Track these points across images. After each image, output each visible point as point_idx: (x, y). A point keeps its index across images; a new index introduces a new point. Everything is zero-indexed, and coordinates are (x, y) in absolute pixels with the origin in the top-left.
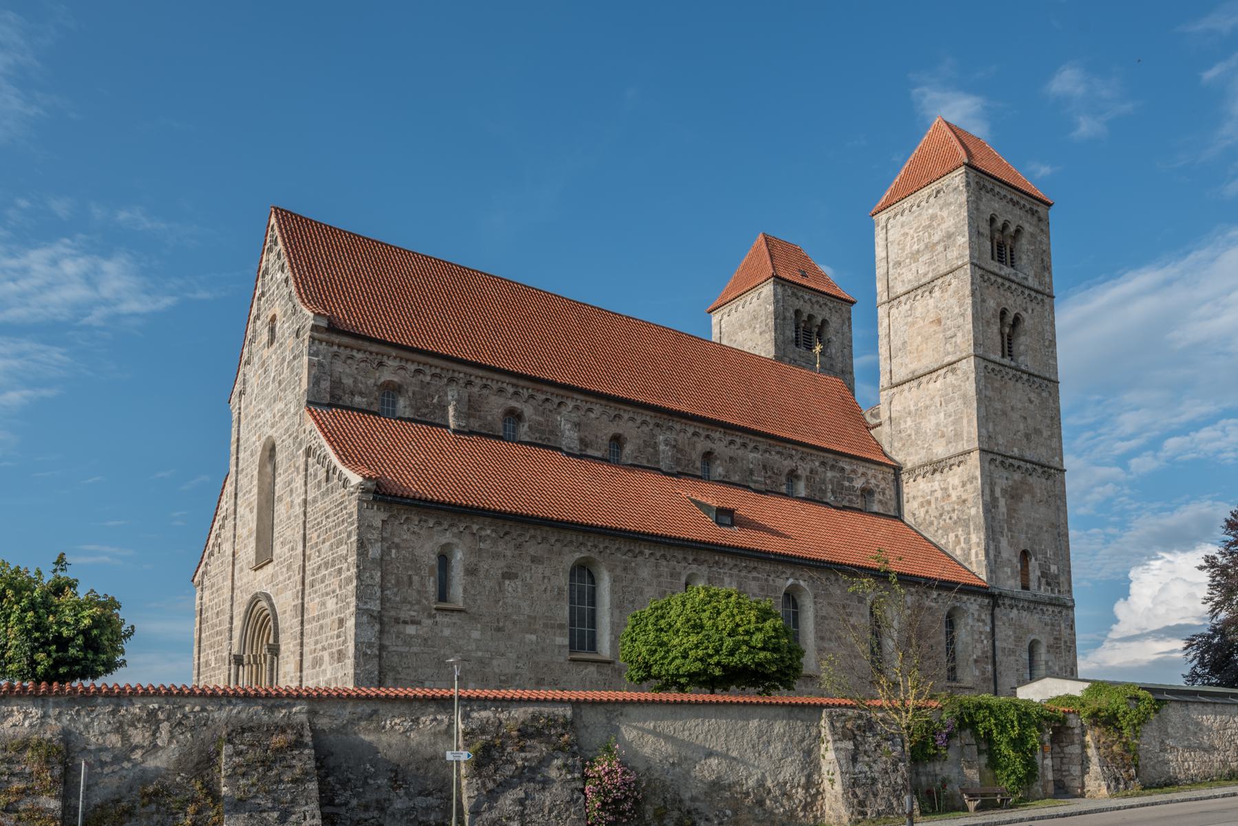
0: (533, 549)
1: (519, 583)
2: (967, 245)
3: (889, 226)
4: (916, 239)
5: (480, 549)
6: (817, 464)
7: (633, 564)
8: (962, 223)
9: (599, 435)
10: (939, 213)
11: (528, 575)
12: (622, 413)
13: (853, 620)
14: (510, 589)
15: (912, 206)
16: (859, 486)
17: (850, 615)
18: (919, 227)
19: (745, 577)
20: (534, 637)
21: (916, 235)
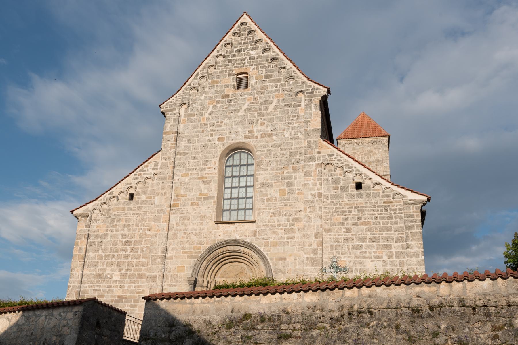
2: (389, 168)
3: (346, 147)
4: (360, 157)
8: (386, 158)
10: (374, 150)
15: (359, 143)
18: (362, 152)
21: (360, 155)
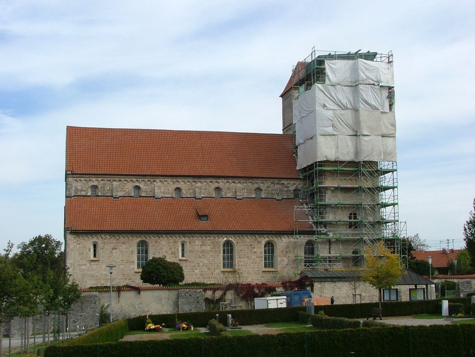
0: (122, 239)
1: (118, 250)
5: (105, 242)
6: (270, 184)
7: (159, 240)
9: (170, 189)
11: (121, 248)
12: (179, 180)
13: (255, 250)
14: (115, 253)
16: (292, 189)
17: (254, 248)
19: (205, 240)
20: (123, 266)
